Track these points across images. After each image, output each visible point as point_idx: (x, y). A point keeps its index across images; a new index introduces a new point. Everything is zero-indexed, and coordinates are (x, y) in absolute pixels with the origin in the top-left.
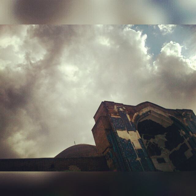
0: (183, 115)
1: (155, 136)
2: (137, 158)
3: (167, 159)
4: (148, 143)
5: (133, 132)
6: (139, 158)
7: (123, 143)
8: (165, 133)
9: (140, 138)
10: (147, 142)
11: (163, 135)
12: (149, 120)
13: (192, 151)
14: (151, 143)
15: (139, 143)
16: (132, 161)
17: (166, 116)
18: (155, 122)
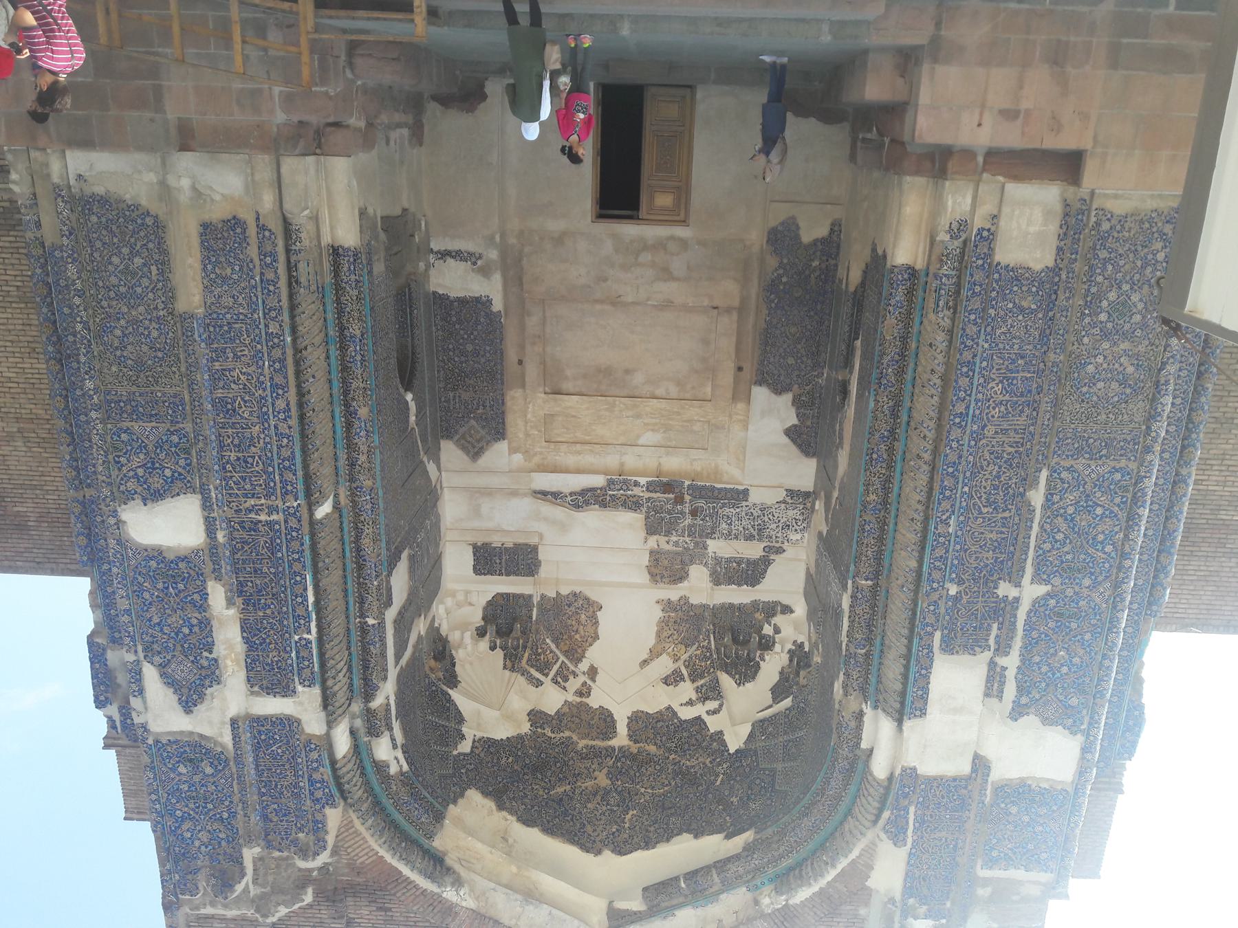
0: (310, 891)
1: (526, 728)
2: (1035, 602)
3: (456, 562)
4: (574, 684)
5: (929, 767)
6: (1017, 600)
7: (1074, 701)
8: (465, 747)
9: (878, 732)
10: (584, 692)
11: (479, 735)
12: (598, 853)
13: (389, 603)
14: (556, 683)
15: (933, 695)
16: (1087, 582)
17: (482, 883)
18: (549, 830)
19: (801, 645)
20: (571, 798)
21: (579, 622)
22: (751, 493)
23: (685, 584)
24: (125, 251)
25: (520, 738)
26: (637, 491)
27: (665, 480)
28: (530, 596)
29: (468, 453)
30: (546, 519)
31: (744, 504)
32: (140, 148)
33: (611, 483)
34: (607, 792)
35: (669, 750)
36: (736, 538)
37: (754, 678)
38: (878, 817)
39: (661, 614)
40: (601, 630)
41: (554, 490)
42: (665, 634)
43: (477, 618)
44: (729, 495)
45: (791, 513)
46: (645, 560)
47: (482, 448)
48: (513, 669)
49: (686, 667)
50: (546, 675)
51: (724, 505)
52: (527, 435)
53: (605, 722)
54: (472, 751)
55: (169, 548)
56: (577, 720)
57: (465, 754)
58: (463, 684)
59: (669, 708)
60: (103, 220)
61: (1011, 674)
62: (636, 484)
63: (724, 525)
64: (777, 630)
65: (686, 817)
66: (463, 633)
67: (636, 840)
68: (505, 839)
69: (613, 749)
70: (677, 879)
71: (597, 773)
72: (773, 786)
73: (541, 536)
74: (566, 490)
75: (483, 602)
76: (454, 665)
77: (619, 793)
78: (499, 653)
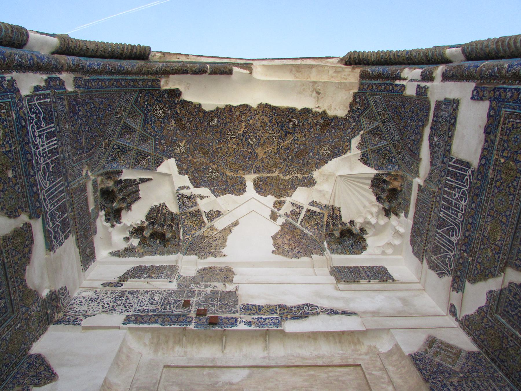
1: (316, 174)
3: (404, 265)
4: (286, 208)
8: (355, 142)
10: (278, 205)
11: (348, 154)
12: (260, 105)
14: (299, 207)
18: (291, 110)
19: (108, 220)
20: (279, 138)
21: (289, 245)
22: (122, 321)
23: (200, 267)
25: (318, 166)
26: (248, 318)
27: (217, 328)
28: (332, 253)
29: (441, 342)
30: (336, 299)
31: (130, 314)
33: (277, 323)
34: (257, 144)
35: (217, 171)
36: (147, 292)
37: (152, 209)
39: (222, 250)
40: (271, 241)
41: (336, 317)
42: (220, 242)
43: (370, 240)
44: (147, 319)
45: (84, 308)
46: (236, 279)
47: (430, 347)
48: (333, 208)
49: (203, 222)
50: (308, 211)
51: (154, 311)
52: (384, 369)
53: (261, 187)
54: (350, 142)
56: (281, 187)
57: (354, 136)
58: (367, 187)
59: (217, 196)
62: (249, 323)
63: (157, 298)
64: (127, 239)
65: (206, 123)
66: (377, 222)
67: (238, 114)
68: (318, 93)
69: (255, 172)
71: (265, 156)
72: (145, 120)
73: (337, 289)
74: (324, 317)
75: (369, 250)
76: (379, 199)
77: (249, 144)
78: (345, 219)
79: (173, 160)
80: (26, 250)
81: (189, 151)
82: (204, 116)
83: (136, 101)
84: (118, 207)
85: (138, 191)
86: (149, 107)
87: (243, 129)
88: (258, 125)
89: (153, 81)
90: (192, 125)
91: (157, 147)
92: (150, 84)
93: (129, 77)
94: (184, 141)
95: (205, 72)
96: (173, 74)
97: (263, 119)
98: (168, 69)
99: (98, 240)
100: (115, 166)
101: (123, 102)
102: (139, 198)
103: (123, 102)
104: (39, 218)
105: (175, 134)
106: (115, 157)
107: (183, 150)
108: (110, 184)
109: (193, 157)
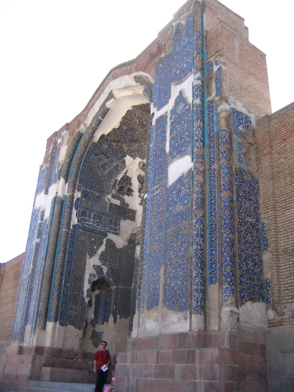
24: (176, 288)
32: (166, 335)
38: (62, 166)
55: (179, 159)
60: (181, 301)
61: (39, 219)
67: (129, 117)
70: (103, 117)
79: (127, 156)
80: (112, 244)
81: (128, 146)
82: (120, 130)
83: (96, 155)
84: (127, 189)
85: (128, 176)
86: (101, 150)
87: (137, 121)
88: (140, 115)
89: (92, 145)
90: (119, 136)
91: (118, 158)
92: (92, 146)
93: (86, 154)
94: (124, 145)
95: (101, 121)
96: (94, 133)
97: (139, 112)
98: (91, 136)
99: (131, 207)
100: (113, 180)
101: (94, 162)
102: (131, 178)
103: (94, 162)
104: (107, 235)
105: (118, 146)
106: (110, 177)
107: (127, 148)
108: (117, 187)
109: (133, 147)
